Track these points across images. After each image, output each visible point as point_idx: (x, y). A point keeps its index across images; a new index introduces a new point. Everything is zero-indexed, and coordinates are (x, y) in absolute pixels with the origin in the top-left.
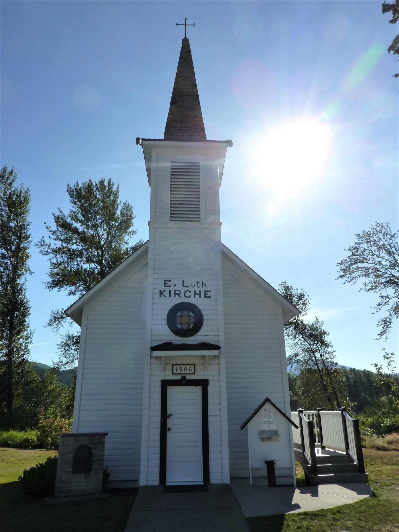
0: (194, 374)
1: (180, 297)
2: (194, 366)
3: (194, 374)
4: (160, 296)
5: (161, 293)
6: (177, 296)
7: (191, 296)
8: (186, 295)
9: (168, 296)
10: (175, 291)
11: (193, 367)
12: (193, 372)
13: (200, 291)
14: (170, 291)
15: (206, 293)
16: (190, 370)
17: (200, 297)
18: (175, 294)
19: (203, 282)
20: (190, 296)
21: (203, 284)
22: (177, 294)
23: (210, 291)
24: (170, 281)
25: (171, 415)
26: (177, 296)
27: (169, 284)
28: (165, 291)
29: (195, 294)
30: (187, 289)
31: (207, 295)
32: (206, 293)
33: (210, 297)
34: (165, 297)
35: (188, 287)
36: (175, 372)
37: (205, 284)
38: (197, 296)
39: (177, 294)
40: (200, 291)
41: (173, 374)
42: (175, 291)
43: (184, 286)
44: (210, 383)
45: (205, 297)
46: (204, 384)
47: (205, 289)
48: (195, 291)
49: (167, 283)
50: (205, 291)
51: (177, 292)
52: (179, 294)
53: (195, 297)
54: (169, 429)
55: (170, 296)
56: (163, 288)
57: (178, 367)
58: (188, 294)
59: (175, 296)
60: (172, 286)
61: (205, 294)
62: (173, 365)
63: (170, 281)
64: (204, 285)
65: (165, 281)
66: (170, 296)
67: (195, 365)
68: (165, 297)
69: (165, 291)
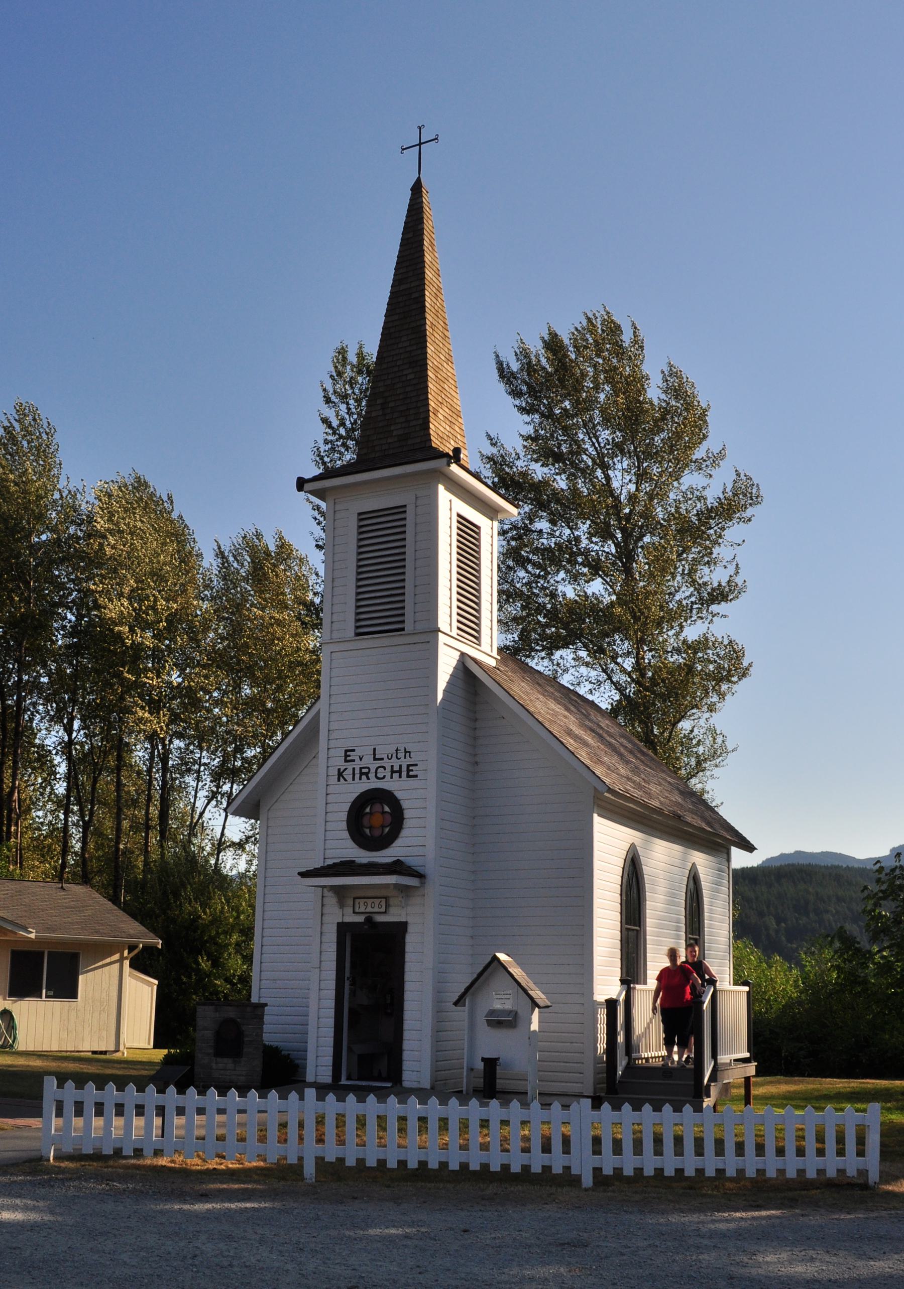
1: (368, 778)
3: (385, 912)
4: (339, 780)
5: (340, 774)
6: (364, 777)
8: (379, 775)
9: (349, 778)
10: (361, 769)
11: (384, 900)
12: (383, 910)
13: (400, 766)
14: (354, 769)
16: (380, 906)
17: (400, 777)
18: (361, 774)
19: (405, 749)
20: (384, 777)
21: (406, 752)
23: (416, 765)
24: (354, 750)
26: (364, 777)
27: (353, 756)
28: (346, 769)
29: (393, 772)
30: (379, 763)
31: (411, 773)
33: (416, 776)
34: (345, 780)
35: (382, 759)
36: (357, 910)
37: (409, 752)
38: (396, 775)
39: (364, 773)
40: (400, 766)
41: (354, 912)
42: (361, 769)
43: (375, 759)
44: (410, 929)
45: (408, 776)
47: (408, 761)
48: (392, 767)
49: (349, 756)
50: (408, 766)
51: (364, 770)
52: (367, 774)
55: (354, 779)
59: (360, 779)
60: (357, 759)
61: (408, 771)
62: (354, 899)
63: (354, 750)
64: (408, 754)
65: (346, 751)
66: (354, 779)
67: (386, 898)
68: (345, 780)
69: (346, 769)
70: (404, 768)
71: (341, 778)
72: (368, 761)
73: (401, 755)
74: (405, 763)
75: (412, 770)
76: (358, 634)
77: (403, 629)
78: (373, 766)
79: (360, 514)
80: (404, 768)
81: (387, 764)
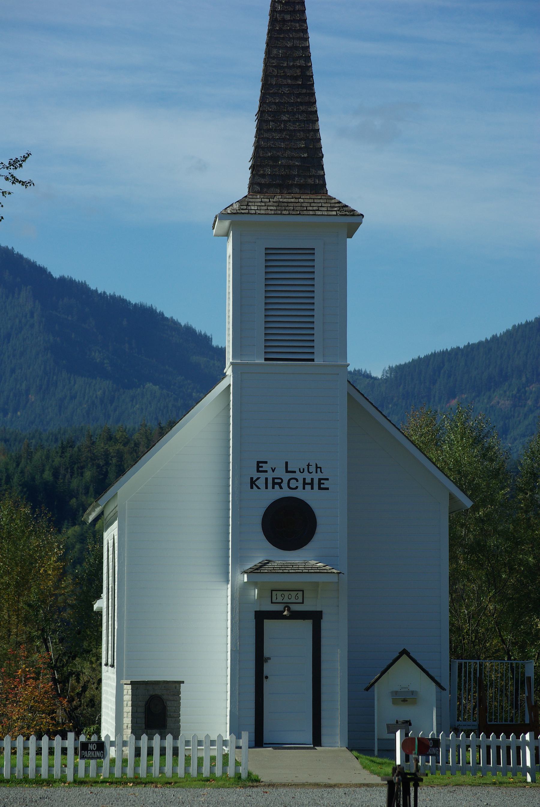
0: (303, 603)
1: (281, 488)
2: (302, 592)
5: (253, 483)
6: (277, 487)
7: (298, 486)
8: (291, 486)
10: (274, 479)
12: (300, 600)
13: (312, 479)
14: (266, 479)
15: (322, 481)
16: (296, 597)
17: (312, 488)
18: (274, 484)
19: (316, 465)
20: (297, 488)
21: (317, 467)
22: (277, 483)
23: (327, 479)
24: (266, 462)
25: (269, 659)
26: (277, 487)
27: (265, 467)
28: (258, 478)
29: (305, 484)
31: (322, 486)
32: (322, 481)
33: (327, 489)
34: (259, 488)
35: (295, 472)
36: (274, 600)
37: (320, 468)
38: (308, 487)
39: (277, 483)
40: (312, 479)
41: (272, 603)
42: (274, 479)
43: (287, 471)
45: (320, 488)
47: (320, 475)
48: (304, 479)
49: (262, 467)
50: (320, 480)
51: (276, 481)
52: (280, 484)
53: (304, 488)
54: (267, 677)
55: (267, 488)
56: (255, 475)
57: (279, 593)
58: (293, 484)
59: (273, 488)
60: (270, 471)
61: (320, 484)
63: (266, 462)
64: (319, 470)
65: (258, 463)
66: (267, 488)
68: (259, 488)
69: (258, 478)
71: (254, 486)
73: (313, 469)
74: (316, 477)
75: (323, 484)
76: (266, 359)
77: (313, 360)
78: (286, 477)
79: (266, 249)
81: (298, 475)
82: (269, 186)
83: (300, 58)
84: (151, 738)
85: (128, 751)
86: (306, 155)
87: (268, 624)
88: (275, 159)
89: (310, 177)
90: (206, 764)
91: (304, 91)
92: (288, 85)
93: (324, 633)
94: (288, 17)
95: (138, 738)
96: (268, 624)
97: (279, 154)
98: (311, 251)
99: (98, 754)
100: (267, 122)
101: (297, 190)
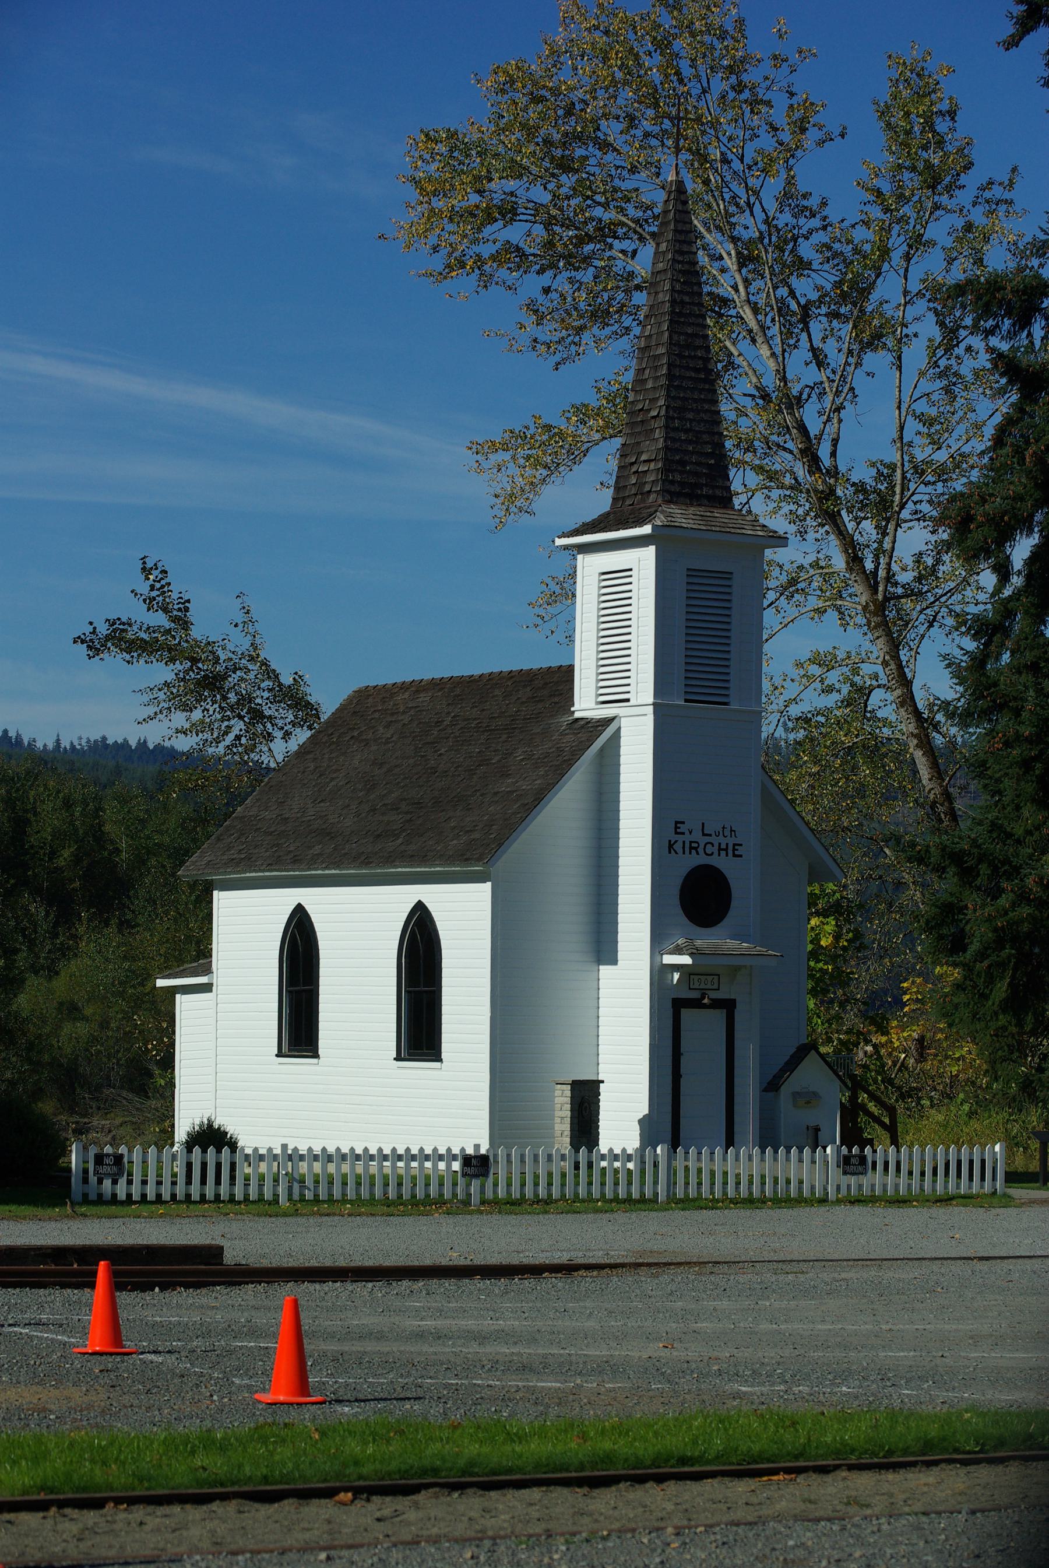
1: (698, 853)
5: (671, 846)
6: (693, 851)
9: (680, 851)
10: (691, 842)
11: (716, 978)
18: (691, 848)
24: (683, 823)
26: (693, 851)
27: (683, 828)
29: (720, 849)
30: (707, 839)
33: (741, 856)
35: (710, 835)
38: (723, 853)
39: (693, 848)
42: (691, 842)
43: (704, 835)
45: (734, 855)
46: (728, 1006)
48: (720, 844)
50: (734, 845)
51: (693, 845)
52: (696, 849)
56: (674, 837)
57: (696, 978)
58: (709, 847)
60: (687, 832)
61: (734, 850)
63: (683, 823)
65: (677, 823)
70: (730, 848)
72: (697, 836)
74: (731, 841)
76: (686, 701)
80: (730, 848)
82: (679, 494)
83: (700, 347)
84: (204, 1151)
85: (567, 1166)
86: (713, 462)
87: (686, 1014)
88: (682, 463)
89: (717, 487)
90: (609, 1179)
91: (707, 387)
92: (691, 378)
93: (737, 1026)
94: (687, 299)
95: (577, 1151)
96: (686, 1014)
97: (687, 458)
98: (728, 575)
99: (860, 1168)
100: (673, 418)
101: (706, 502)
